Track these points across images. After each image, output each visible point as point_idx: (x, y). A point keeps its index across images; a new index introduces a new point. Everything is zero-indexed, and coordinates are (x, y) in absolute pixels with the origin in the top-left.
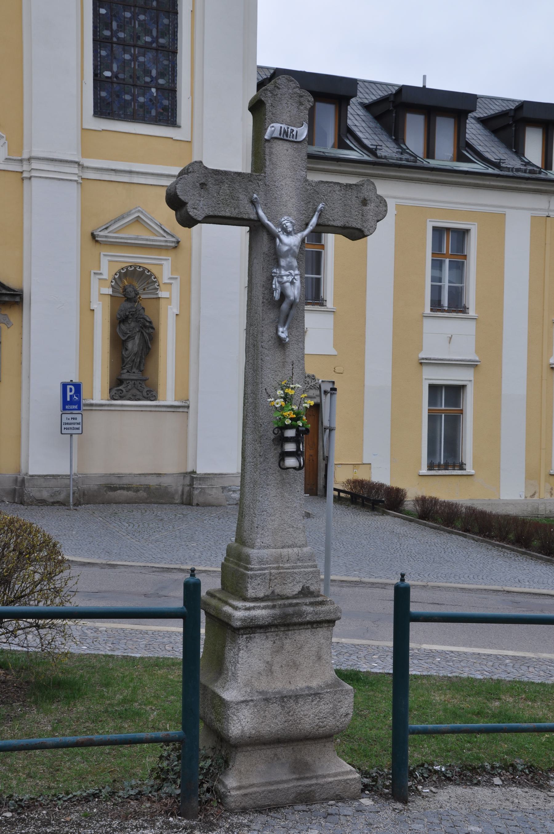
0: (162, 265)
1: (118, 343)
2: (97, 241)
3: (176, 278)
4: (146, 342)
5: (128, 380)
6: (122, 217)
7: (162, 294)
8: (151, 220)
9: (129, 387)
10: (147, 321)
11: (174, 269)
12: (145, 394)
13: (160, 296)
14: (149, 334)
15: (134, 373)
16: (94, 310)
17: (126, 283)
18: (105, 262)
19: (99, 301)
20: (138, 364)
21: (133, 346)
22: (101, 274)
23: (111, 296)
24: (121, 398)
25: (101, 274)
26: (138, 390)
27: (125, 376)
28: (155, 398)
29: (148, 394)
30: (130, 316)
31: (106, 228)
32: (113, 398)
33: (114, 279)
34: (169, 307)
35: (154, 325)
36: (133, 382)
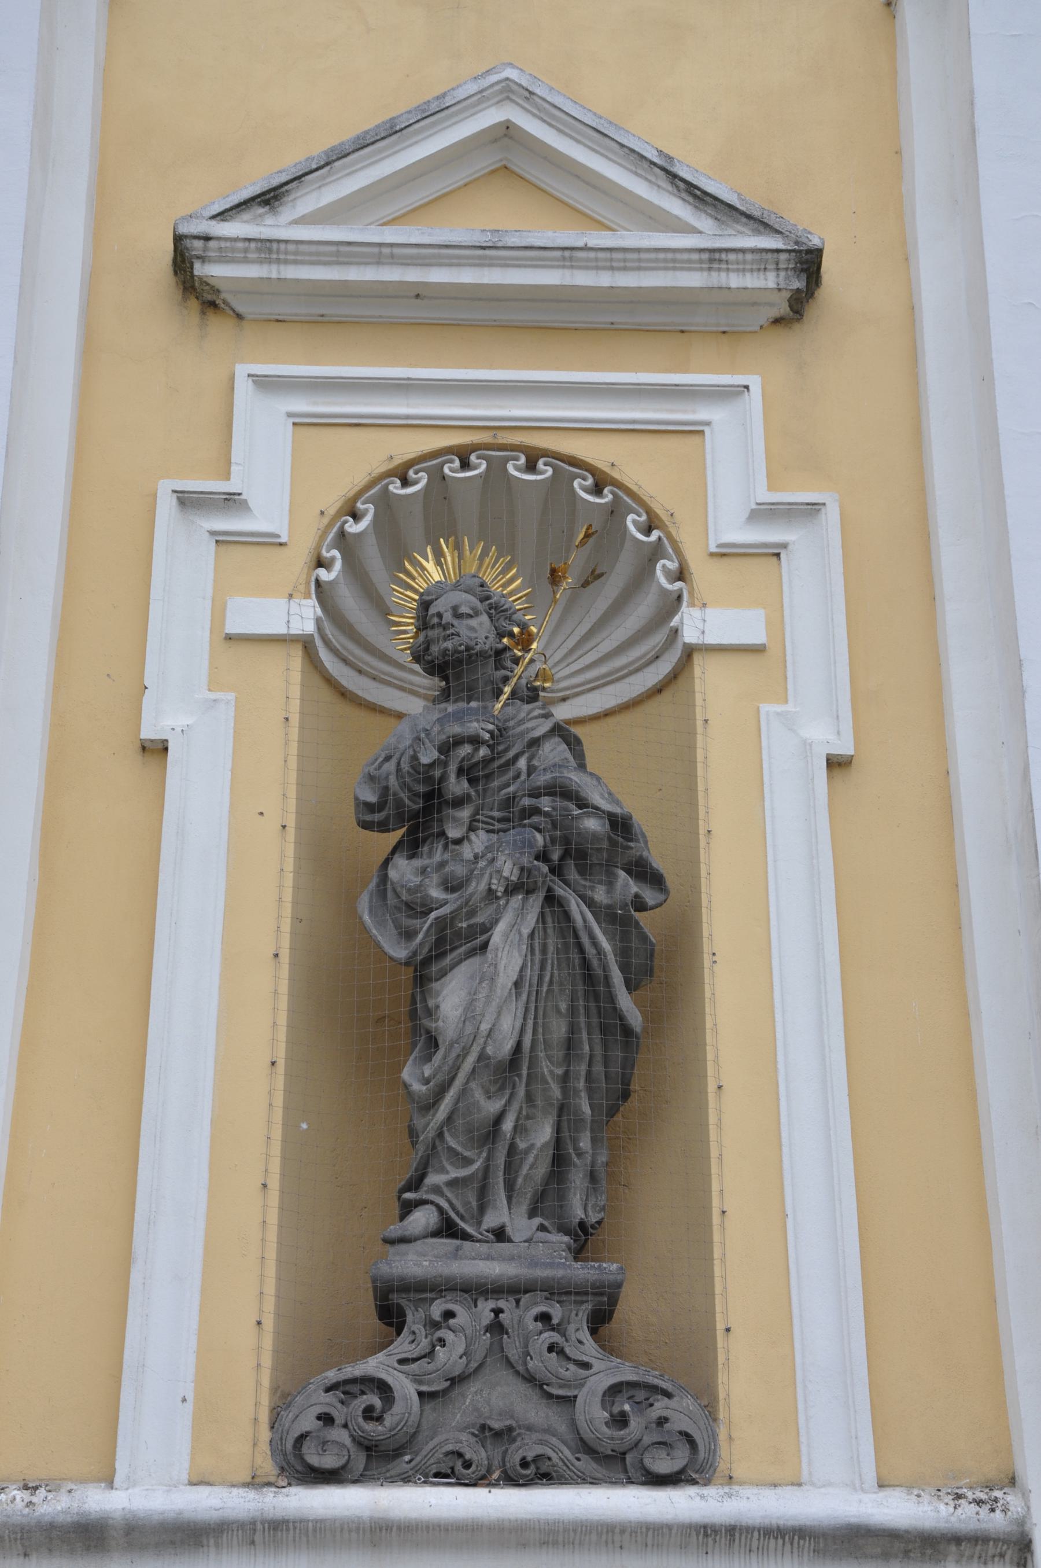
0: (695, 432)
1: (368, 998)
3: (814, 509)
4: (591, 980)
6: (393, 132)
8: (599, 136)
9: (450, 1357)
11: (791, 449)
13: (690, 636)
14: (620, 921)
15: (500, 1235)
16: (162, 748)
20: (535, 1169)
21: (484, 999)
22: (232, 502)
24: (381, 1459)
25: (232, 502)
26: (529, 1378)
27: (419, 1262)
29: (621, 1421)
30: (457, 786)
31: (270, 198)
36: (485, 1308)
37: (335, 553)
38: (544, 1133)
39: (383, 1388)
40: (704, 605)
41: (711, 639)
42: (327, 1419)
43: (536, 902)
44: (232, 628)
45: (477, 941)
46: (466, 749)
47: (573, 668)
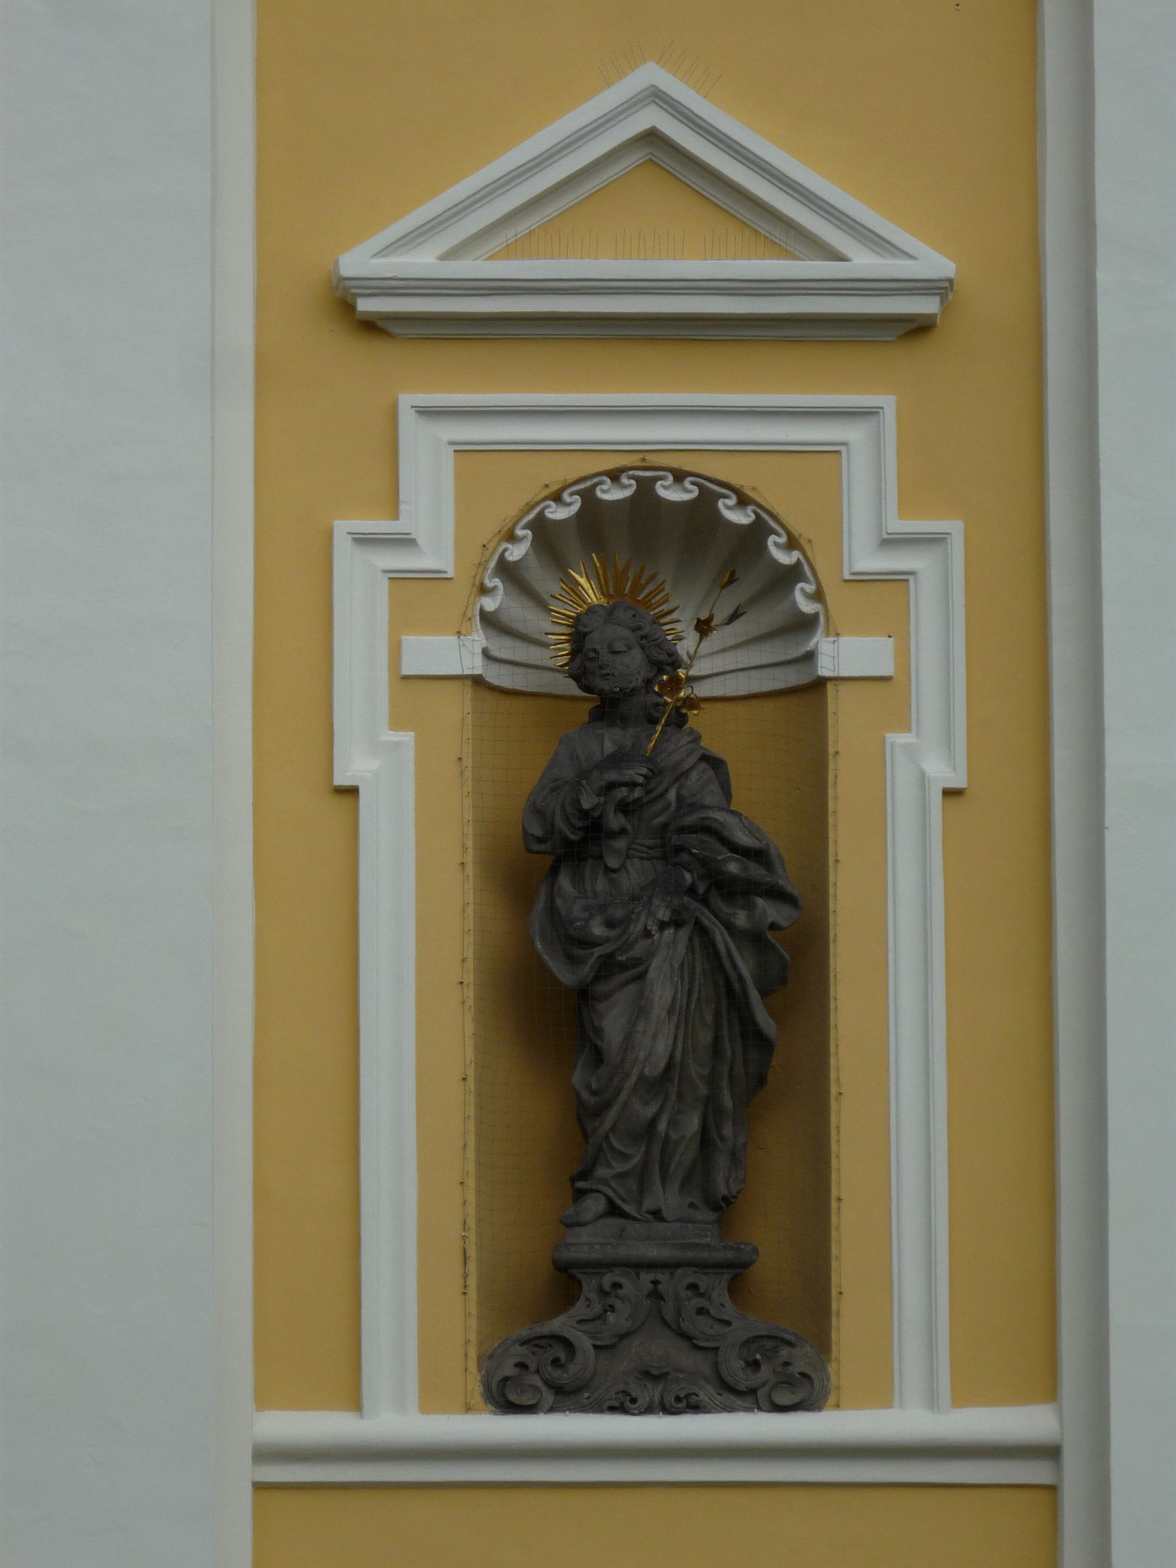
2: (372, 326)
4: (733, 998)
5: (611, 1265)
7: (842, 654)
9: (617, 1321)
10: (735, 848)
12: (734, 1368)
13: (825, 668)
14: (756, 940)
16: (352, 792)
17: (592, 595)
18: (428, 462)
19: (398, 722)
20: (685, 1155)
22: (405, 542)
23: (477, 681)
24: (568, 1396)
25: (405, 542)
27: (589, 1243)
28: (803, 1390)
29: (755, 1365)
30: (615, 821)
32: (504, 1400)
33: (506, 569)
34: (896, 739)
35: (790, 878)
36: (646, 1278)
37: (497, 582)
38: (693, 1123)
39: (567, 1344)
40: (838, 635)
41: (844, 673)
42: (522, 1366)
43: (684, 933)
44: (406, 670)
45: (637, 971)
46: (622, 792)
47: (719, 664)
